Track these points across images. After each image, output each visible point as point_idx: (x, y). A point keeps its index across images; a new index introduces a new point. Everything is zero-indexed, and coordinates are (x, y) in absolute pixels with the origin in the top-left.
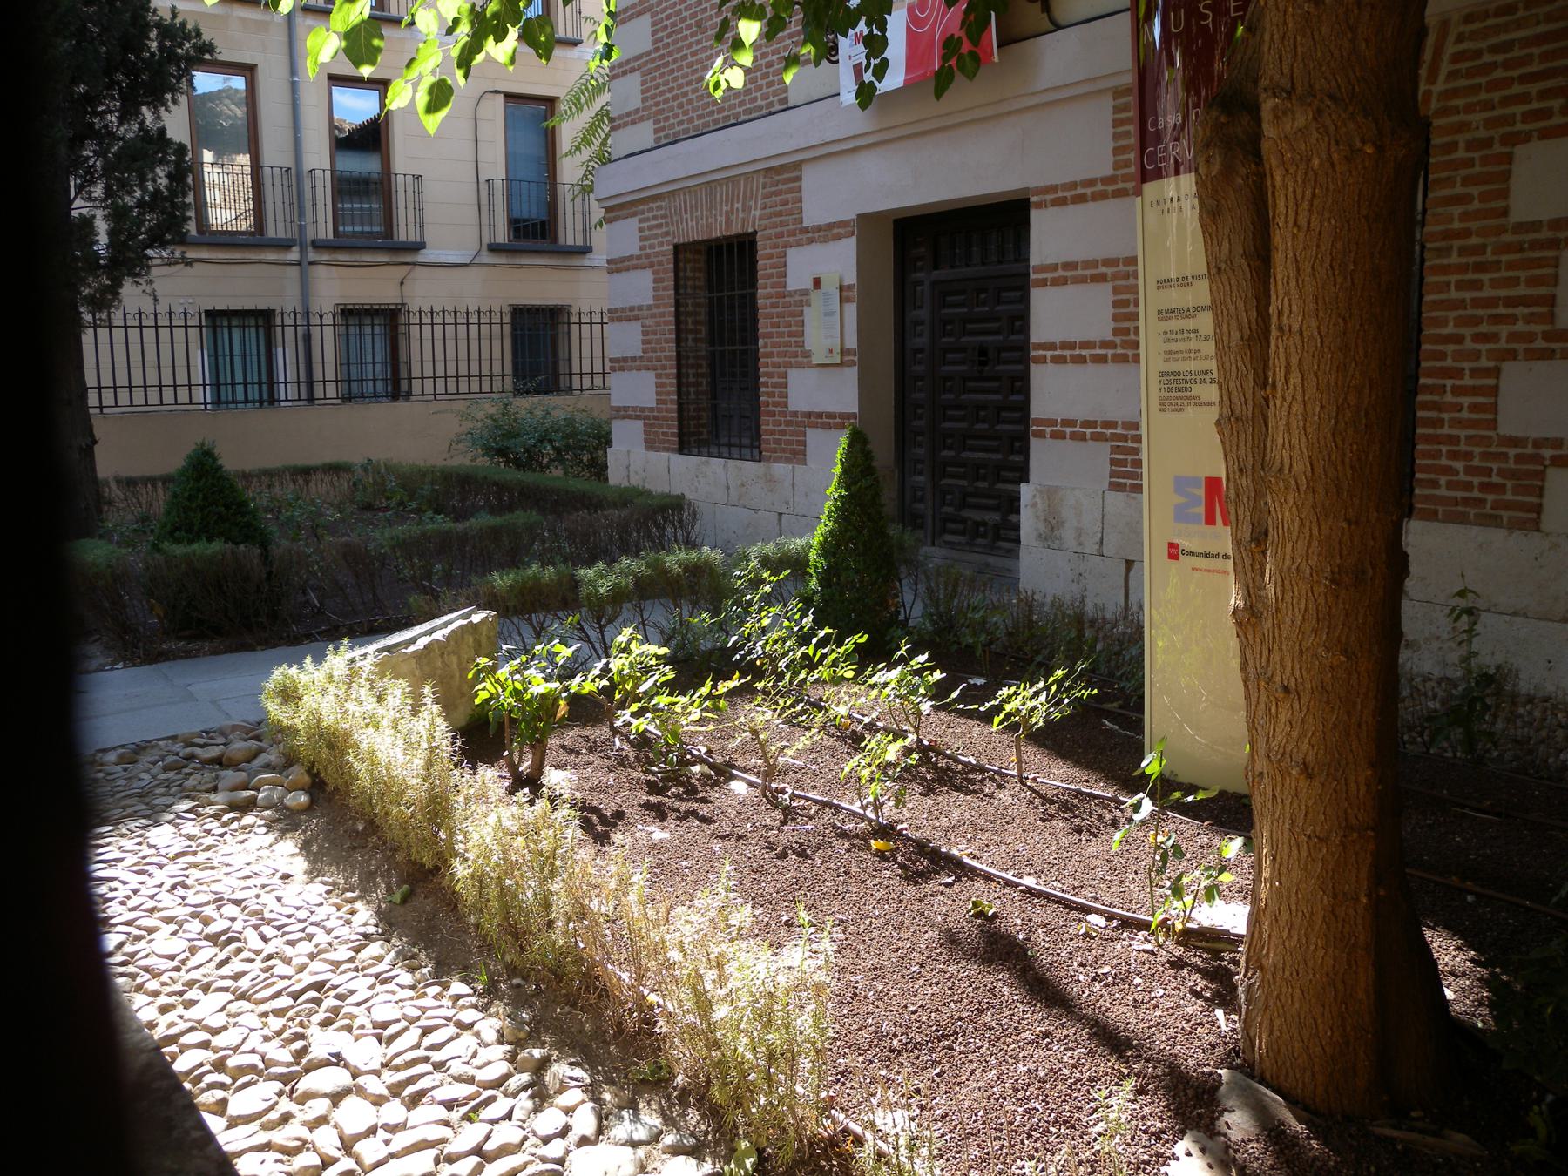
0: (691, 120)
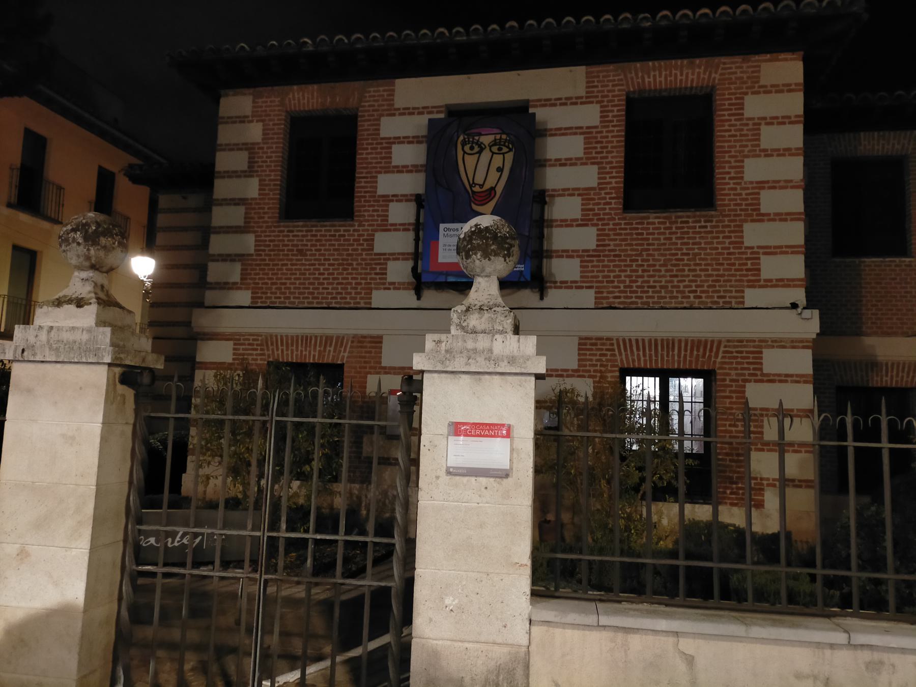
0: (289, 298)
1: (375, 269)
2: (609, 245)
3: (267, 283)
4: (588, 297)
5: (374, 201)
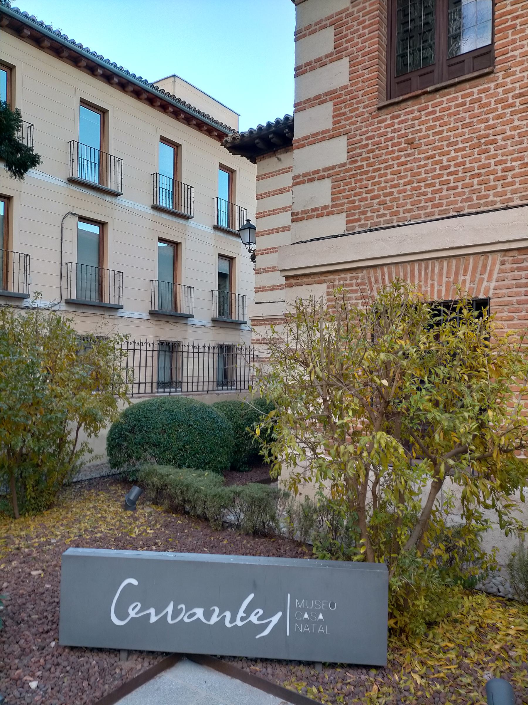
0: (397, 213)
3: (366, 199)
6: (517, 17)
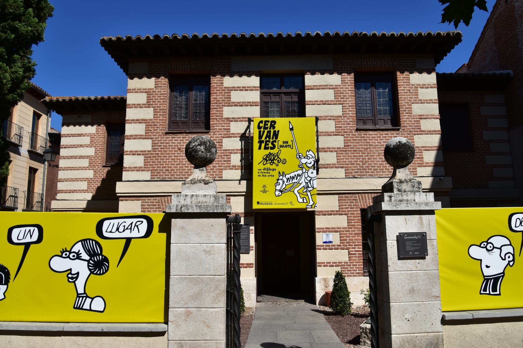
0: (173, 175)
1: (224, 158)
2: (351, 145)
3: (160, 167)
4: (341, 172)
5: (222, 121)
6: (218, 116)
